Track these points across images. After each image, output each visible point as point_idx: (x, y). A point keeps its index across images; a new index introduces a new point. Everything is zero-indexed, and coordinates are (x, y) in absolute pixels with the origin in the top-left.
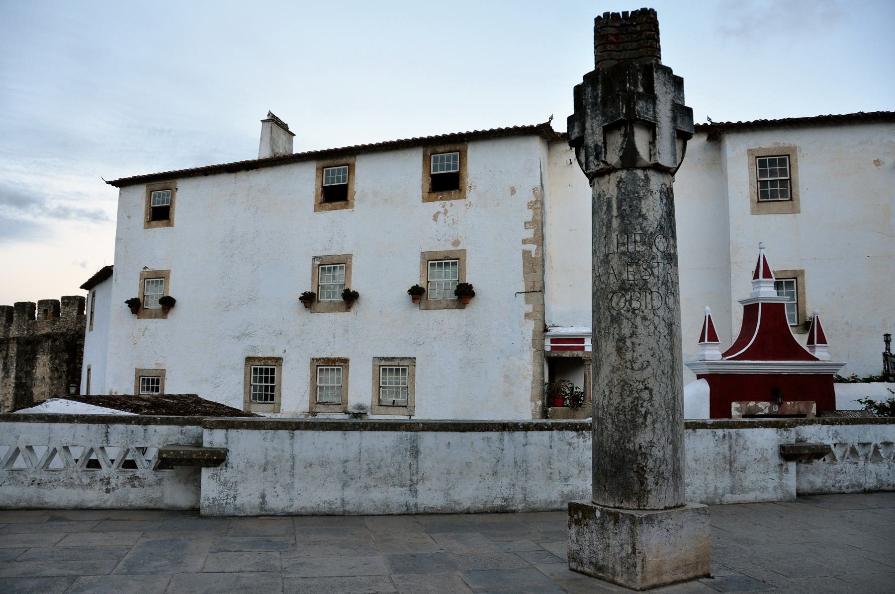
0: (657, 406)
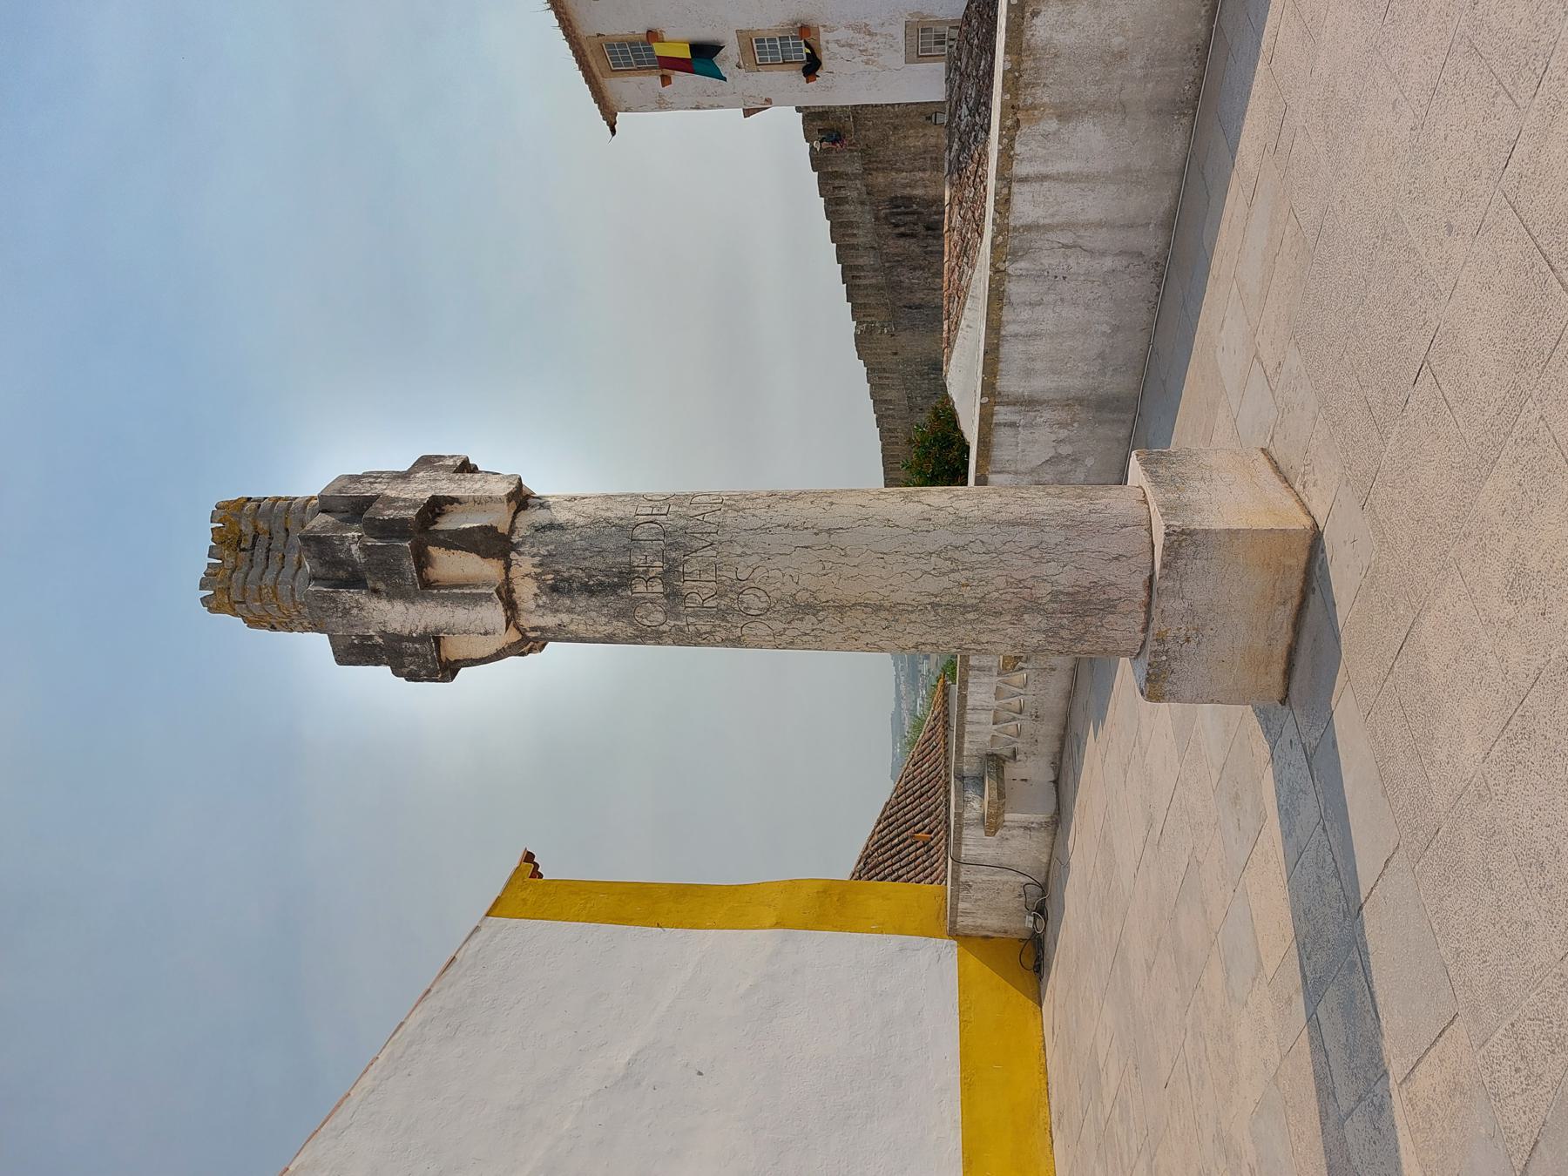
0: (947, 639)
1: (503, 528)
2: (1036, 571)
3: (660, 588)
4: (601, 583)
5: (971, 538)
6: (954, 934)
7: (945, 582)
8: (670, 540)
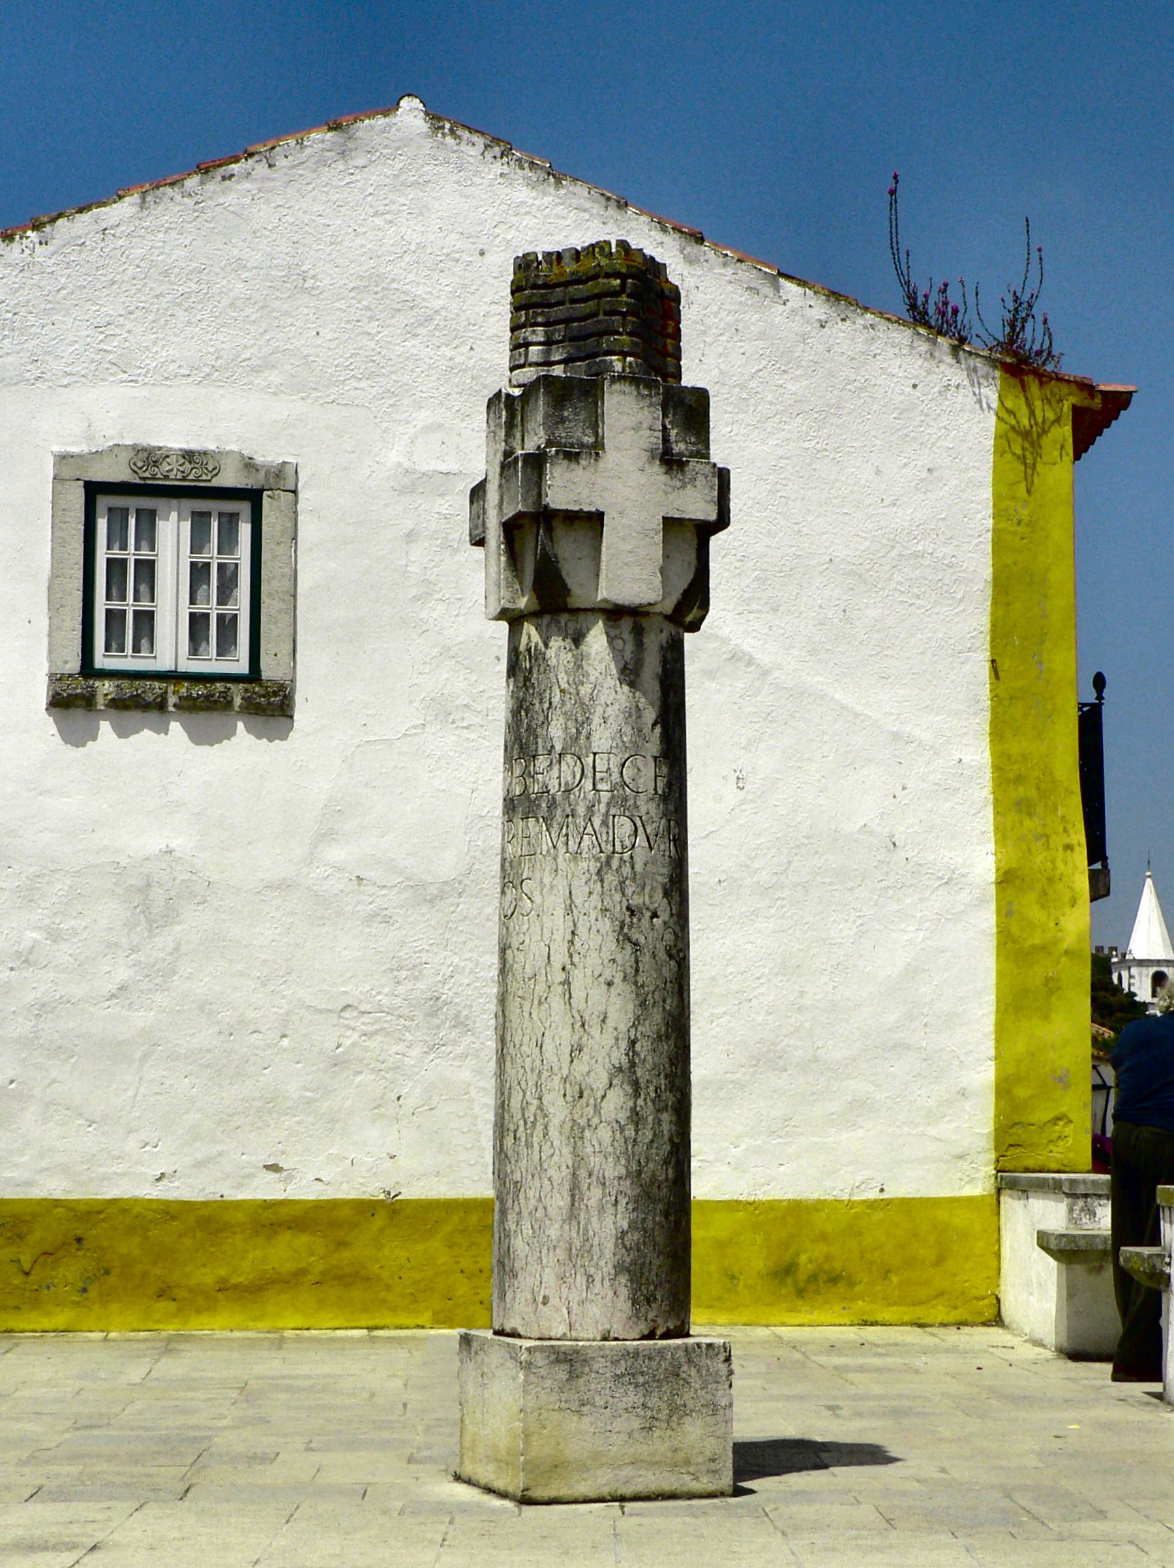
2: (525, 1213)
5: (557, 1143)
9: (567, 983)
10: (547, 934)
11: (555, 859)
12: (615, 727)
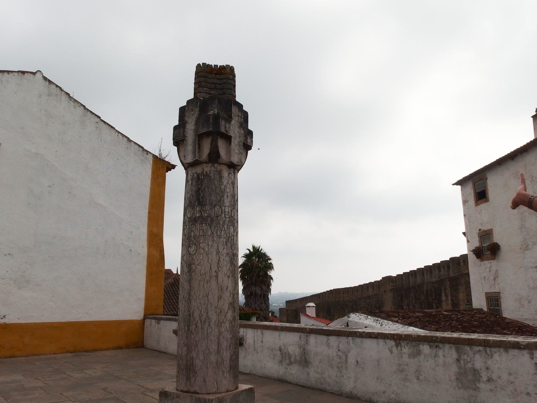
1: (220, 161)
3: (198, 215)
4: (200, 195)
5: (213, 328)
6: (144, 319)
7: (197, 319)
8: (214, 218)
9: (217, 276)
10: (210, 260)
11: (213, 237)
12: (230, 200)
